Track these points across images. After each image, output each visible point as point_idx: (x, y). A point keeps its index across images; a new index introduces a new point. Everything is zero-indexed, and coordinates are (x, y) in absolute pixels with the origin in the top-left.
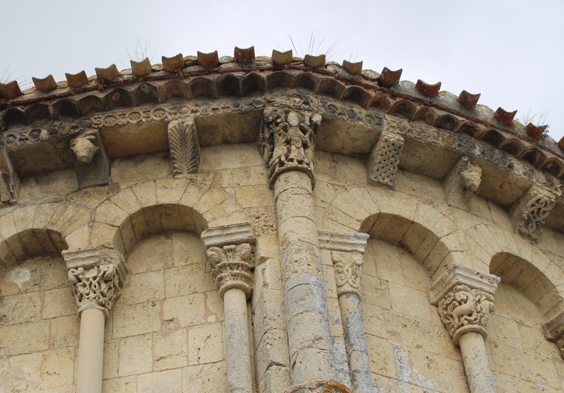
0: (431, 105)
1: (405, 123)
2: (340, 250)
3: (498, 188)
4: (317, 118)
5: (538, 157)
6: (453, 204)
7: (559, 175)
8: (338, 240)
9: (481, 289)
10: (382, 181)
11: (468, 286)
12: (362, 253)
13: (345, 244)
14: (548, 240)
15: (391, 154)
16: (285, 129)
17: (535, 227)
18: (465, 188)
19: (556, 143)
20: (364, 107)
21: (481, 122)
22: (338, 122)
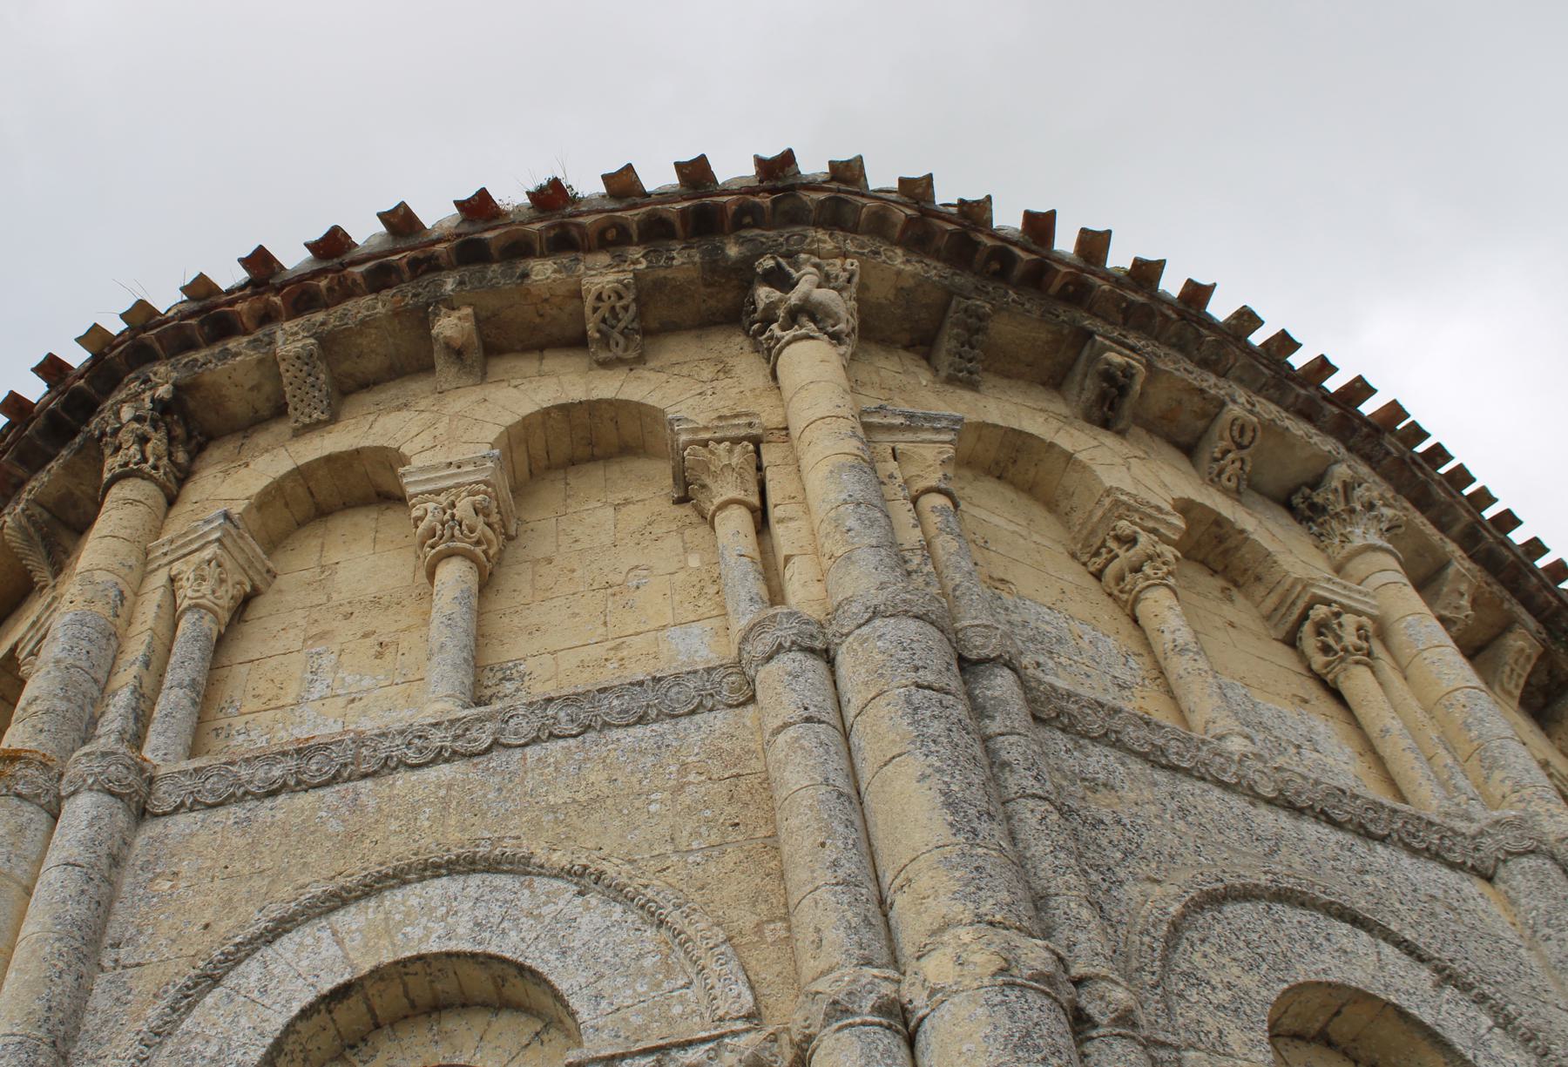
0: (344, 266)
1: (319, 317)
2: (184, 556)
3: (538, 320)
4: (163, 391)
5: (574, 232)
6: (445, 386)
7: (635, 239)
8: (180, 542)
9: (458, 486)
10: (307, 420)
11: (430, 493)
12: (218, 540)
13: (191, 542)
14: (680, 350)
15: (304, 374)
16: (116, 432)
17: (622, 341)
18: (457, 353)
19: (604, 196)
20: (246, 333)
21: (439, 240)
22: (207, 378)
